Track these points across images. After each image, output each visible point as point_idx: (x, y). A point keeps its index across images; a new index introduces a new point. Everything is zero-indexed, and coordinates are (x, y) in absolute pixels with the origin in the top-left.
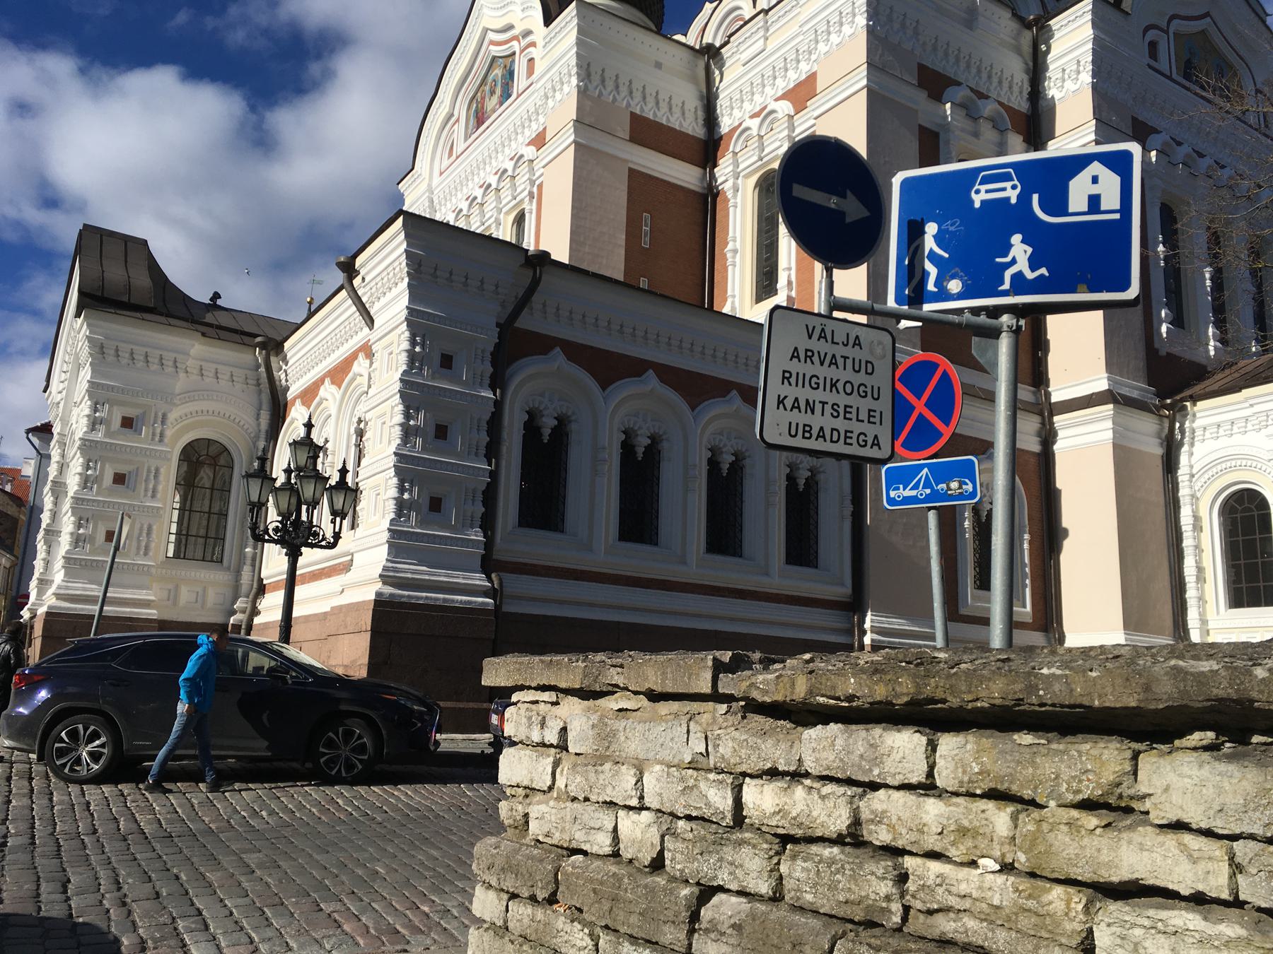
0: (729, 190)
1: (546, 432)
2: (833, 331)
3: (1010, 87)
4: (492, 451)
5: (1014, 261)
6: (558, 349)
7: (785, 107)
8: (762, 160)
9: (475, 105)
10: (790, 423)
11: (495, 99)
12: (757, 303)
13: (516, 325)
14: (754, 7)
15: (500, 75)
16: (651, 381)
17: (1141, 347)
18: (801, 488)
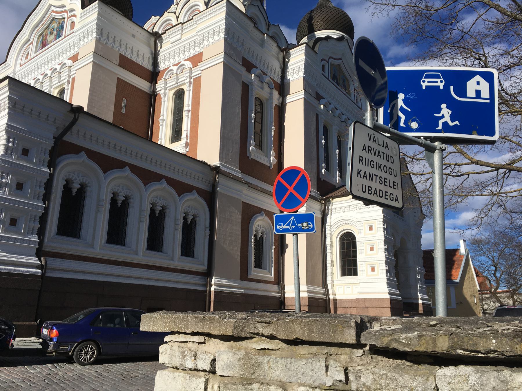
0: (162, 94)
1: (74, 191)
2: (378, 138)
3: (275, 73)
4: (46, 198)
5: (443, 116)
6: (83, 152)
7: (188, 64)
8: (177, 84)
9: (42, 38)
10: (363, 185)
11: (53, 37)
12: (171, 143)
13: (63, 139)
14: (177, 21)
15: (56, 27)
16: (127, 171)
17: (316, 177)
18: (189, 223)
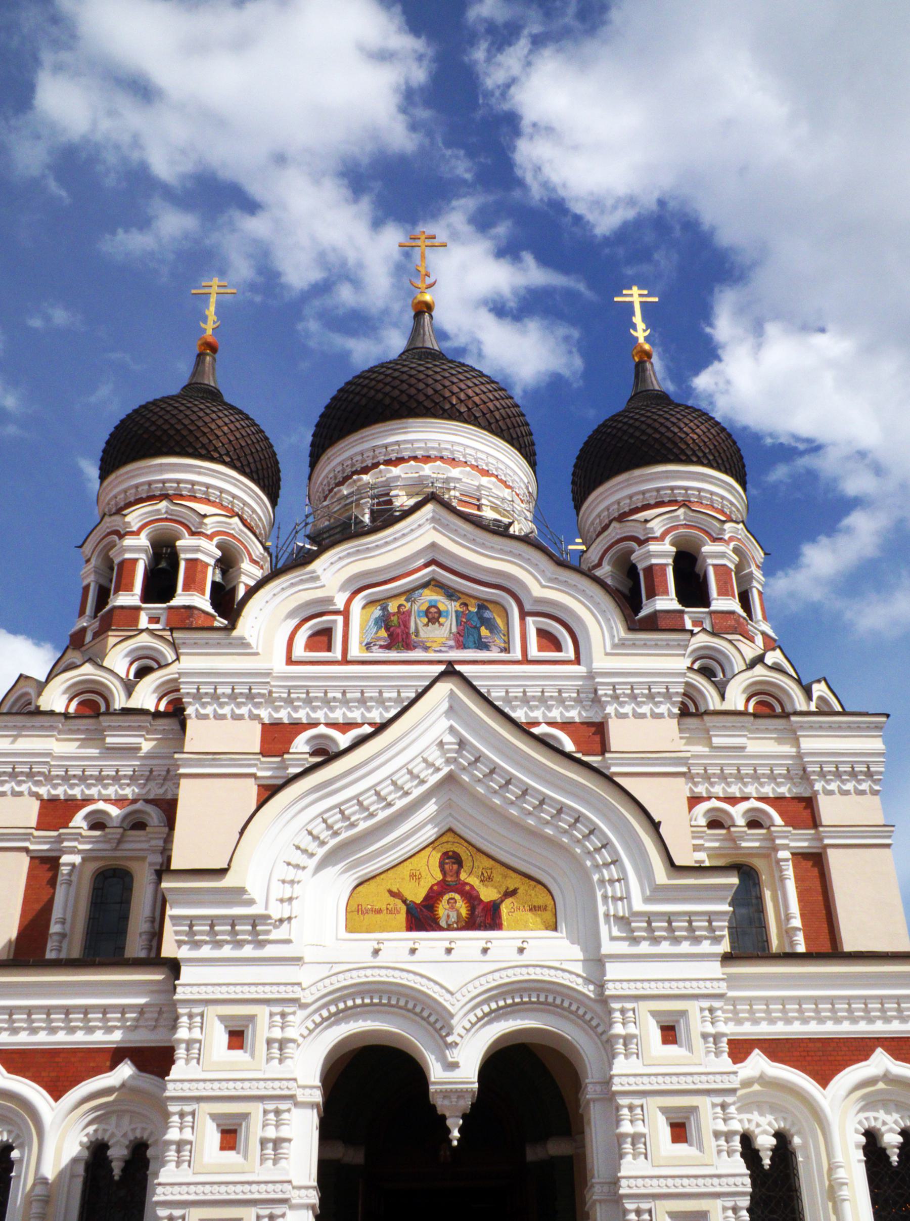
9: (377, 612)
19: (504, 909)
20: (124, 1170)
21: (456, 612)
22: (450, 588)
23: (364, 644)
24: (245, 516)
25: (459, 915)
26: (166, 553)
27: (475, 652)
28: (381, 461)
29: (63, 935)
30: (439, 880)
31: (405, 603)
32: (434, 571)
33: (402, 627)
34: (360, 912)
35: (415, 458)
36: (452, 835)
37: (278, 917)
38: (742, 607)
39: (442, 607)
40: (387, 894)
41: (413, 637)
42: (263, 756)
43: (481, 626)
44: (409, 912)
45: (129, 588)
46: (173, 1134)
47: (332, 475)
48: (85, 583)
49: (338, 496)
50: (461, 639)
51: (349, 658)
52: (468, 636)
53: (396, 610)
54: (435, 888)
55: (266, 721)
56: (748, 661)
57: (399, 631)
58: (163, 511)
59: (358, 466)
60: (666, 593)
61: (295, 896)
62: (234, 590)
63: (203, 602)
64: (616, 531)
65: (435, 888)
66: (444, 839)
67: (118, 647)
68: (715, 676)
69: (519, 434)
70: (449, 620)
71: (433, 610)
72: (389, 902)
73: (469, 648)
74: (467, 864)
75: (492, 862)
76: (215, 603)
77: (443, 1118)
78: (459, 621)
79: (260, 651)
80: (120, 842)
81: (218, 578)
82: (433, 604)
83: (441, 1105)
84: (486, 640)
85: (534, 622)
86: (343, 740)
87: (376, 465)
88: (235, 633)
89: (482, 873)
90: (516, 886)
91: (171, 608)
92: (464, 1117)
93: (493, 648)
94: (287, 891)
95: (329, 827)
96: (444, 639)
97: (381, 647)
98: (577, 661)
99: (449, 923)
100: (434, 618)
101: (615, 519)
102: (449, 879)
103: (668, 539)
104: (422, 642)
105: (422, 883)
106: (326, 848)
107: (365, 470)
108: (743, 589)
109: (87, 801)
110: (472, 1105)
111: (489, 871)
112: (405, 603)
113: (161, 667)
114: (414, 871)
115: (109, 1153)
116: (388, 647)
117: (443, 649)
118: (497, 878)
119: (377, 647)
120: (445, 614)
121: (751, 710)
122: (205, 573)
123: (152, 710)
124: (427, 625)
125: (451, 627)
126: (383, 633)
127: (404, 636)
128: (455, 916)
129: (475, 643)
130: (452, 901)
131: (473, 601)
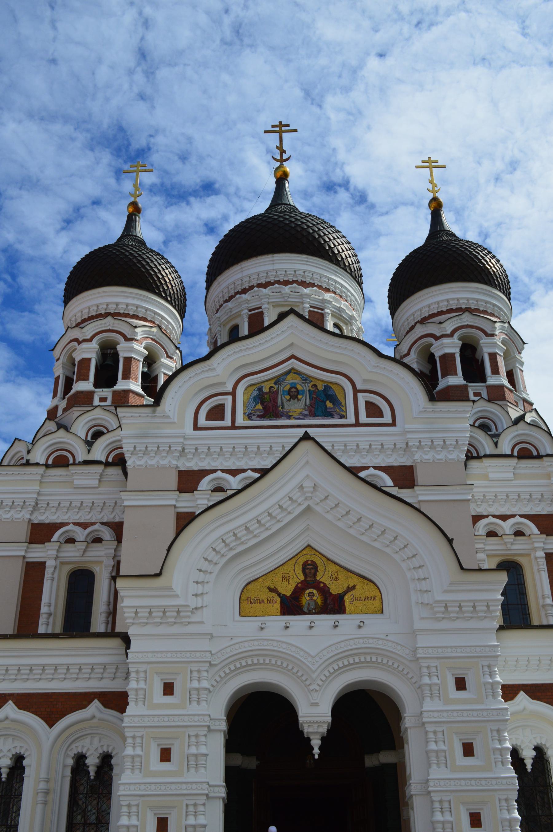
7: (531, 528)
9: (256, 393)
19: (347, 599)
20: (97, 773)
21: (309, 391)
22: (304, 374)
23: (246, 415)
24: (163, 327)
25: (316, 603)
26: (110, 353)
27: (323, 419)
28: (255, 285)
29: (50, 614)
30: (302, 580)
31: (274, 385)
32: (293, 363)
33: (272, 402)
34: (249, 603)
35: (279, 282)
36: (311, 548)
37: (194, 607)
38: (509, 382)
39: (299, 388)
40: (268, 590)
41: (280, 409)
42: (180, 492)
43: (327, 400)
44: (282, 603)
45: (86, 378)
46: (129, 751)
47: (221, 295)
48: (56, 375)
49: (226, 309)
50: (313, 409)
51: (237, 425)
52: (318, 407)
53: (268, 391)
54: (300, 585)
55: (182, 469)
56: (513, 420)
57: (270, 405)
58: (107, 324)
59: (239, 289)
60: (456, 374)
61: (205, 592)
62: (156, 378)
63: (136, 386)
64: (420, 330)
65: (300, 585)
66: (305, 552)
67: (80, 418)
68: (490, 431)
69: (351, 263)
70: (305, 396)
71: (293, 390)
72: (269, 595)
73: (318, 416)
74: (321, 569)
75: (338, 567)
76: (143, 388)
77: (309, 740)
78: (311, 397)
79: (176, 420)
80: (85, 551)
81: (146, 370)
82: (293, 385)
83: (306, 729)
84: (330, 410)
85: (363, 397)
86: (235, 483)
87: (251, 288)
88: (159, 409)
89: (332, 575)
90: (355, 583)
91: (114, 392)
92: (322, 739)
93: (335, 415)
94: (199, 589)
95: (227, 545)
96: (301, 410)
97: (258, 416)
98: (393, 423)
99: (309, 609)
100: (294, 395)
101: (418, 322)
102: (309, 579)
103: (456, 335)
104: (287, 412)
105: (291, 582)
106: (225, 559)
107: (244, 291)
108: (509, 369)
109: (62, 525)
110: (328, 731)
111: (336, 574)
112: (274, 385)
113: (108, 432)
114: (285, 574)
115: (87, 761)
116: (263, 417)
117: (301, 417)
118: (341, 577)
119: (255, 416)
120: (301, 392)
121: (515, 454)
122: (138, 366)
123: (104, 461)
124: (289, 400)
125: (306, 402)
126: (259, 407)
127: (274, 409)
128: (314, 605)
129: (323, 412)
130: (311, 594)
131: (321, 383)
